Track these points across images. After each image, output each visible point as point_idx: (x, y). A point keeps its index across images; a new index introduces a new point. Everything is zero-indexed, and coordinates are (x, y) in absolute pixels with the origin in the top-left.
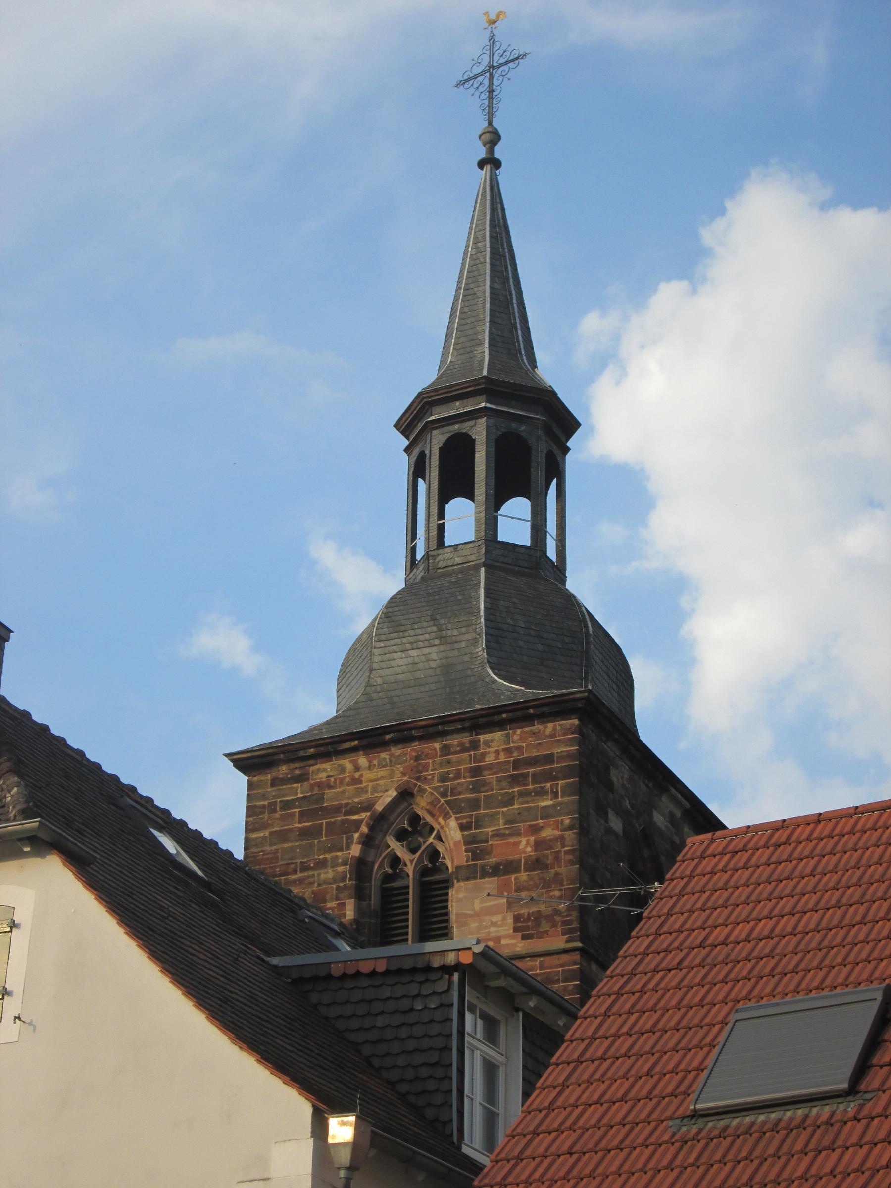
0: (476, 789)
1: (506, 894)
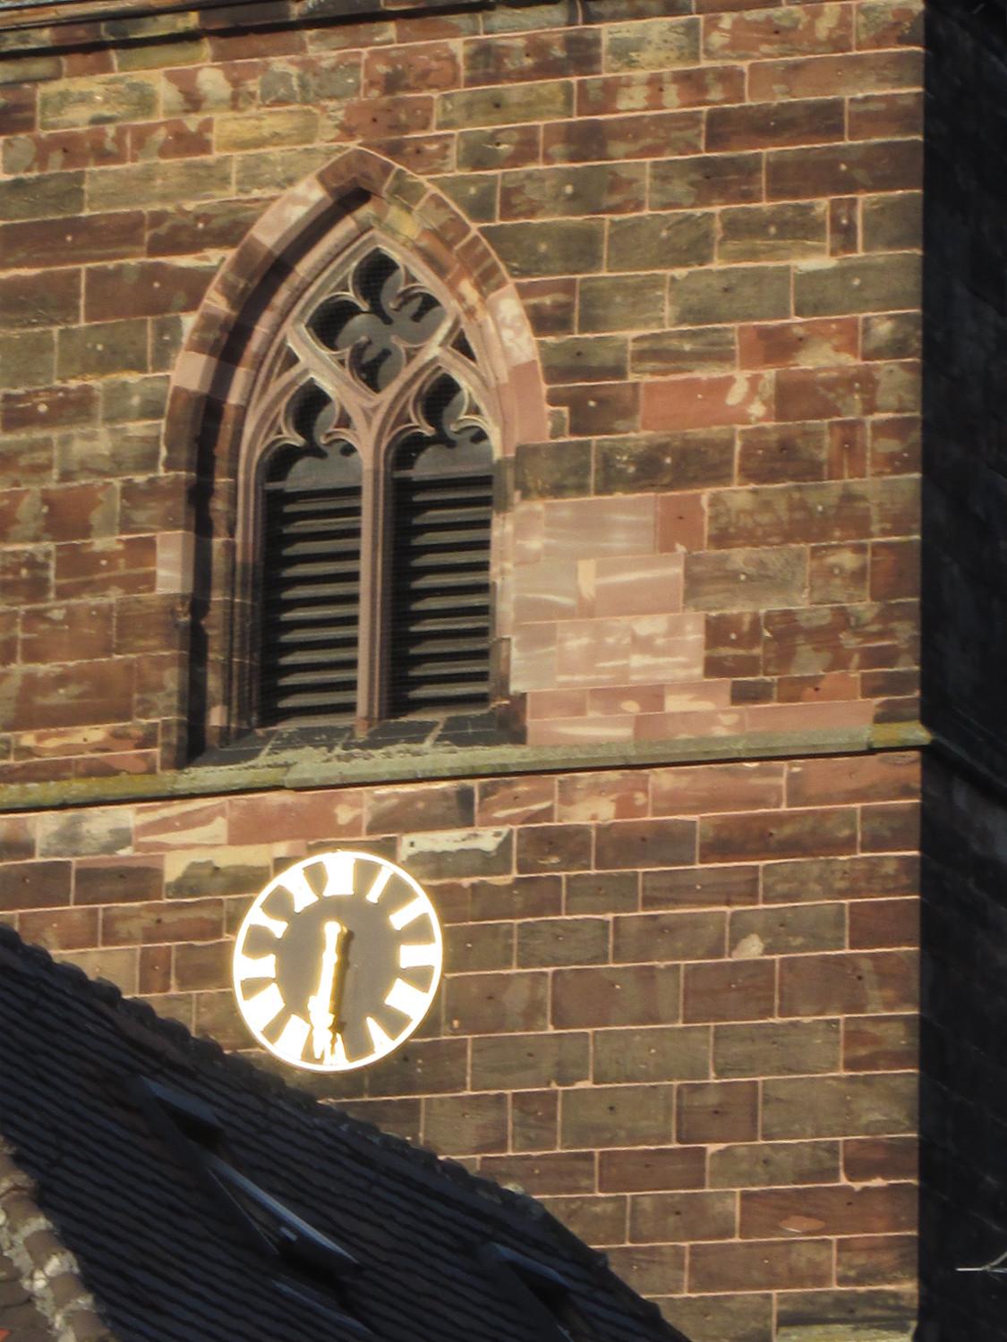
0: (585, 197)
1: (681, 549)
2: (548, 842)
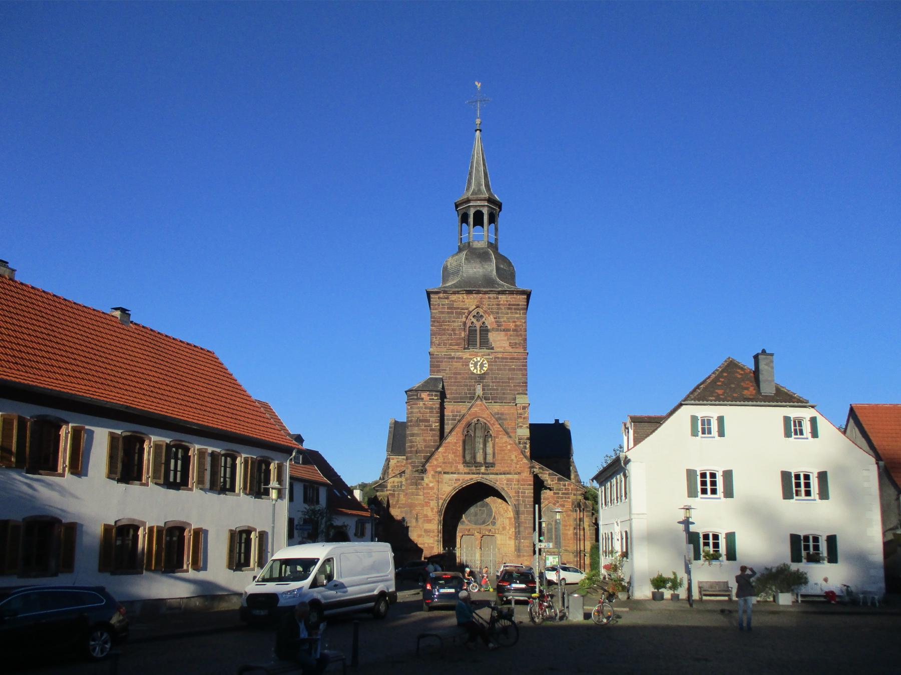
2: (496, 358)
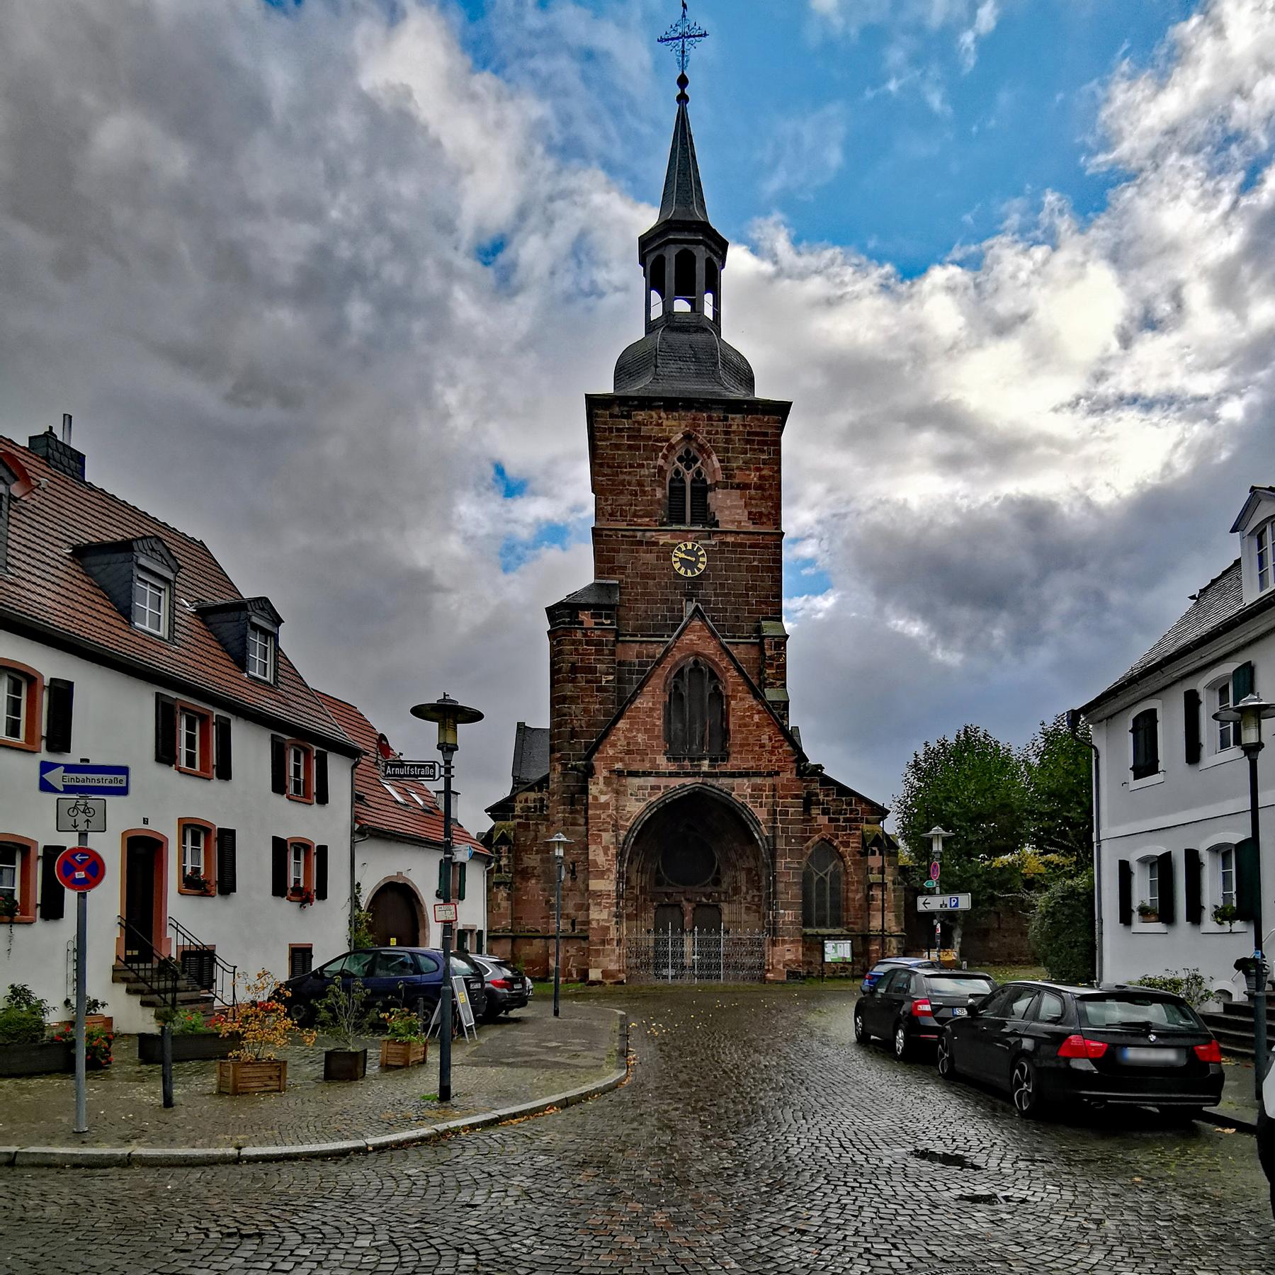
0: (728, 441)
